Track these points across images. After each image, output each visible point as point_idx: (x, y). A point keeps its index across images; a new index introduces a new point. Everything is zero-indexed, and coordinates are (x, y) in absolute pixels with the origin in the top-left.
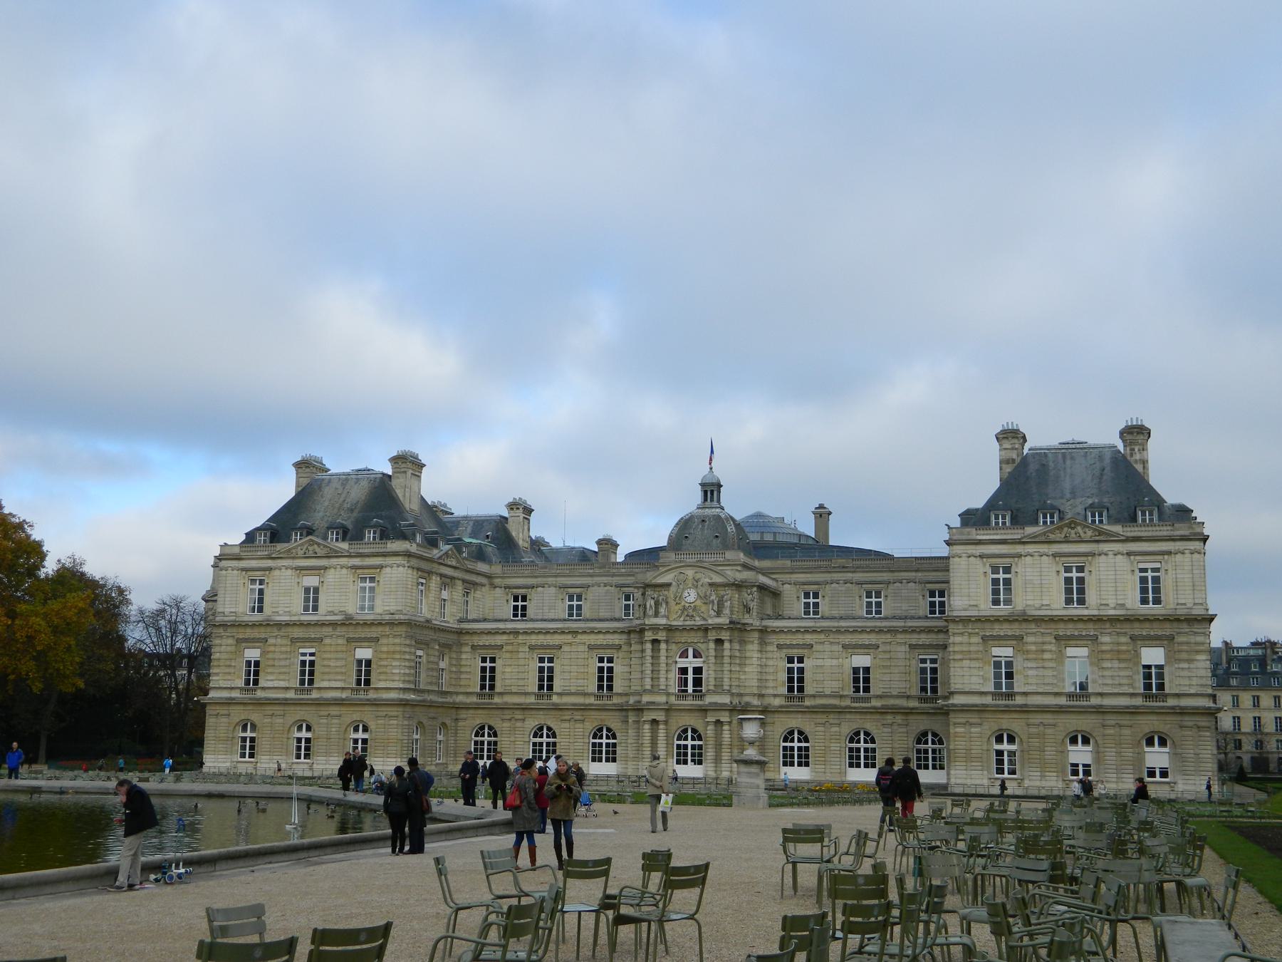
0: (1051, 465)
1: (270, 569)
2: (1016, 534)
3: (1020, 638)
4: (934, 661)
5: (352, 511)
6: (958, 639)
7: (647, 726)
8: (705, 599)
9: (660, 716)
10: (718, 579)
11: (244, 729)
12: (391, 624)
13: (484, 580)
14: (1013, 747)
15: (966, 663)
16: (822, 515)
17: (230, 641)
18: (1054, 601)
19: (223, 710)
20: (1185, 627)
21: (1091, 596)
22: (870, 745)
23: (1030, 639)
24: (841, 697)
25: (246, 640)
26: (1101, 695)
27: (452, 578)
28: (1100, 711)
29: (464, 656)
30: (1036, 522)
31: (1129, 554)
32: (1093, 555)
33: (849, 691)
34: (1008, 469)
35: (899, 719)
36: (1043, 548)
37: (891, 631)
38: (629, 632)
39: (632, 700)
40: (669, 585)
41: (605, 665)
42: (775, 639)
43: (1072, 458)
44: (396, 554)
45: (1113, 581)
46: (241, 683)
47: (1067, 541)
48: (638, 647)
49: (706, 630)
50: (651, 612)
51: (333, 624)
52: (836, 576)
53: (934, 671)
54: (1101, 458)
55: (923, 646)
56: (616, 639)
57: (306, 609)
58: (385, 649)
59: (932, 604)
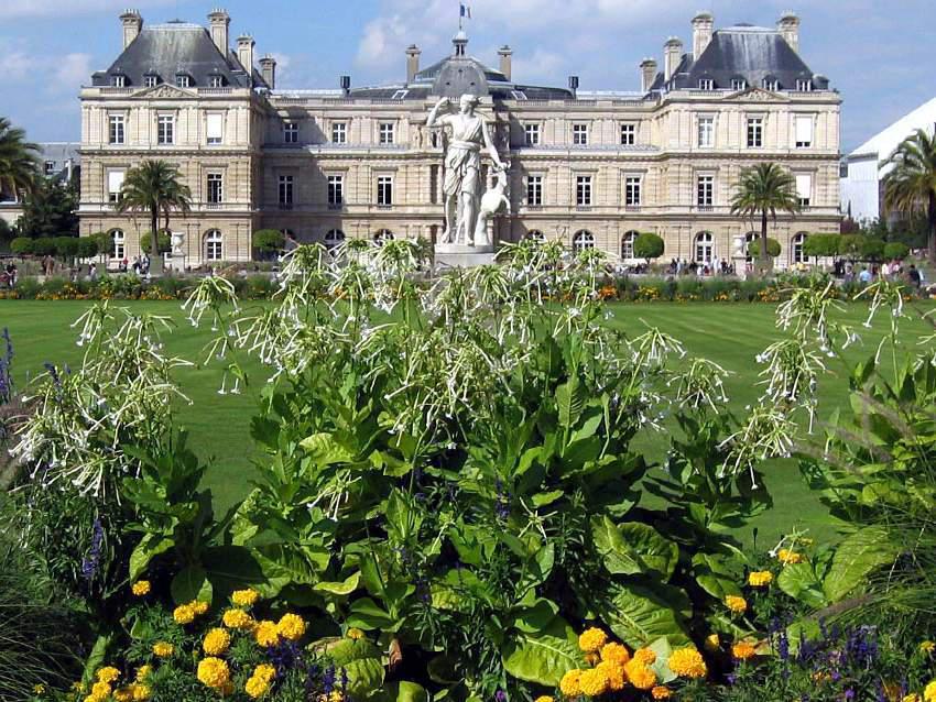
0: (735, 44)
1: (129, 109)
3: (718, 169)
4: (637, 180)
5: (188, 60)
6: (676, 169)
7: (428, 230)
12: (238, 153)
13: (263, 112)
17: (98, 166)
18: (739, 144)
20: (825, 163)
22: (589, 242)
24: (570, 207)
25: (107, 166)
29: (266, 176)
33: (574, 203)
35: (612, 223)
36: (735, 107)
37: (609, 159)
38: (407, 157)
39: (410, 210)
41: (384, 182)
43: (748, 39)
44: (241, 99)
48: (417, 170)
51: (190, 153)
52: (552, 114)
53: (637, 188)
55: (631, 171)
57: (161, 140)
58: (235, 173)
59: (624, 137)
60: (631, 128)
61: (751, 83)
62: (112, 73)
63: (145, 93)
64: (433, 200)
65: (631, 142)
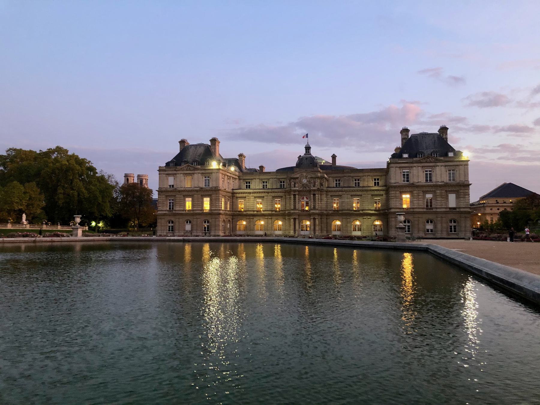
1: (175, 174)
2: (411, 160)
6: (393, 192)
7: (292, 220)
8: (309, 182)
9: (297, 217)
10: (313, 176)
11: (169, 223)
14: (409, 224)
15: (395, 199)
16: (334, 157)
17: (164, 196)
19: (162, 217)
21: (434, 179)
23: (415, 192)
25: (168, 196)
26: (437, 208)
27: (230, 177)
28: (436, 213)
30: (416, 157)
31: (445, 166)
32: (434, 166)
34: (404, 141)
36: (419, 165)
39: (287, 212)
40: (297, 178)
42: (330, 194)
45: (441, 174)
46: (168, 209)
47: (426, 162)
48: (289, 197)
49: (310, 191)
50: (292, 186)
51: (197, 191)
52: (345, 175)
54: (434, 137)
56: (281, 194)
60: (378, 180)
61: (426, 155)
62: (172, 161)
63: (181, 169)
64: (295, 209)
65: (378, 185)
